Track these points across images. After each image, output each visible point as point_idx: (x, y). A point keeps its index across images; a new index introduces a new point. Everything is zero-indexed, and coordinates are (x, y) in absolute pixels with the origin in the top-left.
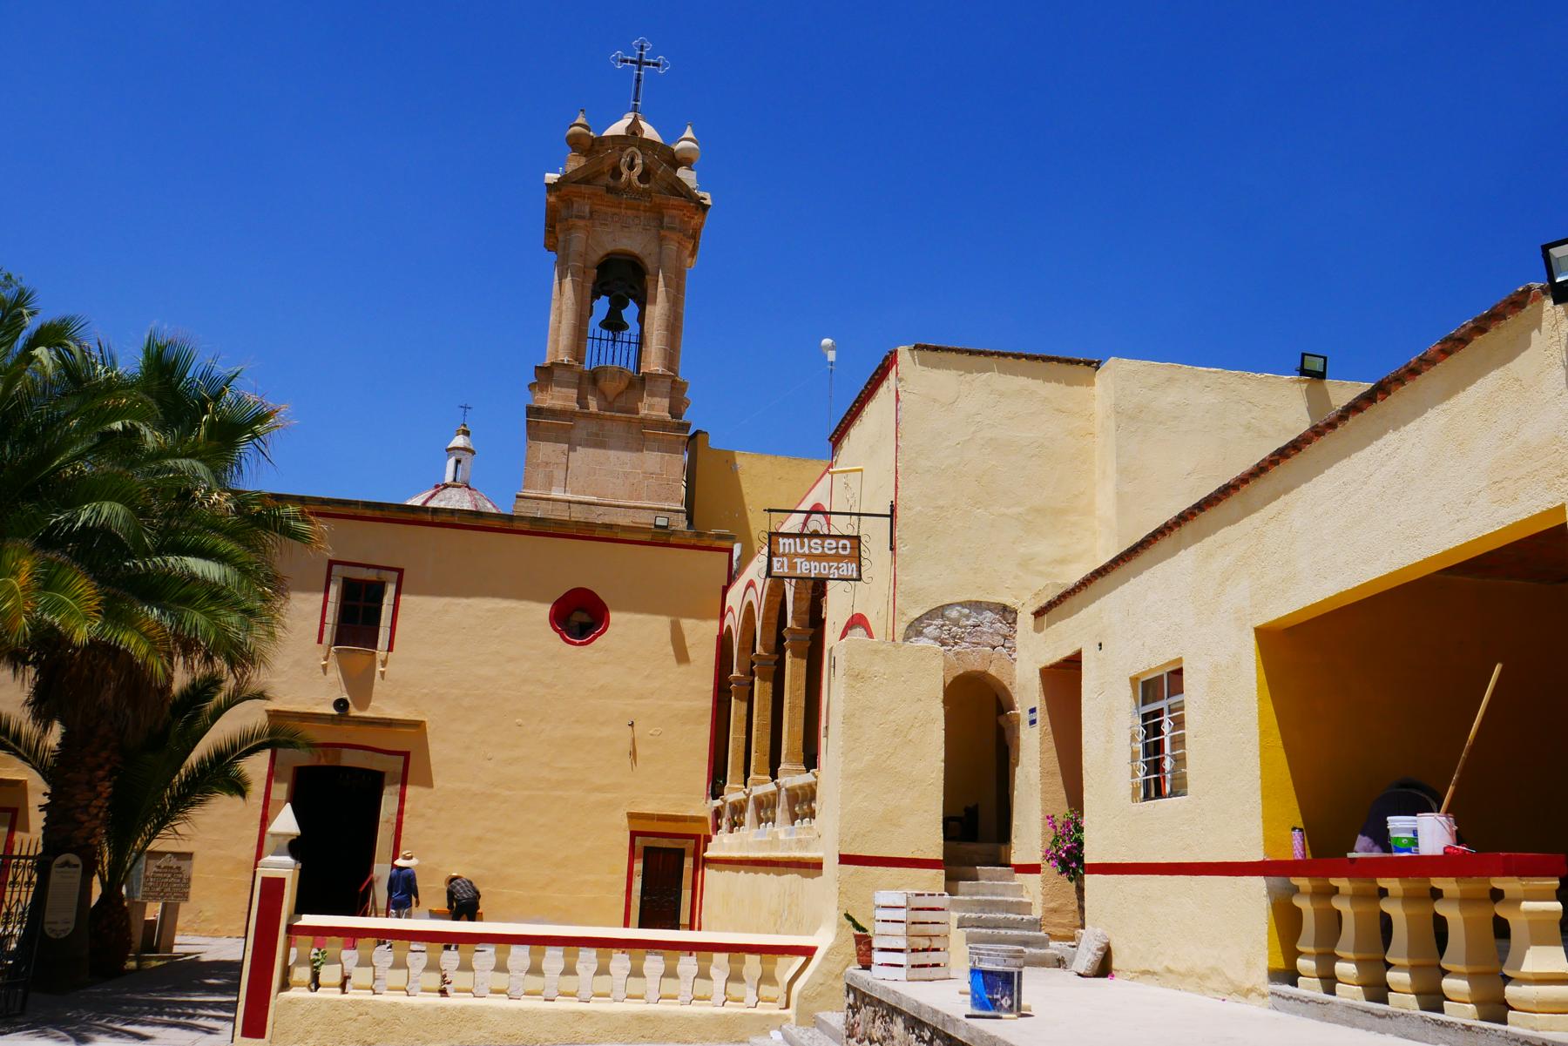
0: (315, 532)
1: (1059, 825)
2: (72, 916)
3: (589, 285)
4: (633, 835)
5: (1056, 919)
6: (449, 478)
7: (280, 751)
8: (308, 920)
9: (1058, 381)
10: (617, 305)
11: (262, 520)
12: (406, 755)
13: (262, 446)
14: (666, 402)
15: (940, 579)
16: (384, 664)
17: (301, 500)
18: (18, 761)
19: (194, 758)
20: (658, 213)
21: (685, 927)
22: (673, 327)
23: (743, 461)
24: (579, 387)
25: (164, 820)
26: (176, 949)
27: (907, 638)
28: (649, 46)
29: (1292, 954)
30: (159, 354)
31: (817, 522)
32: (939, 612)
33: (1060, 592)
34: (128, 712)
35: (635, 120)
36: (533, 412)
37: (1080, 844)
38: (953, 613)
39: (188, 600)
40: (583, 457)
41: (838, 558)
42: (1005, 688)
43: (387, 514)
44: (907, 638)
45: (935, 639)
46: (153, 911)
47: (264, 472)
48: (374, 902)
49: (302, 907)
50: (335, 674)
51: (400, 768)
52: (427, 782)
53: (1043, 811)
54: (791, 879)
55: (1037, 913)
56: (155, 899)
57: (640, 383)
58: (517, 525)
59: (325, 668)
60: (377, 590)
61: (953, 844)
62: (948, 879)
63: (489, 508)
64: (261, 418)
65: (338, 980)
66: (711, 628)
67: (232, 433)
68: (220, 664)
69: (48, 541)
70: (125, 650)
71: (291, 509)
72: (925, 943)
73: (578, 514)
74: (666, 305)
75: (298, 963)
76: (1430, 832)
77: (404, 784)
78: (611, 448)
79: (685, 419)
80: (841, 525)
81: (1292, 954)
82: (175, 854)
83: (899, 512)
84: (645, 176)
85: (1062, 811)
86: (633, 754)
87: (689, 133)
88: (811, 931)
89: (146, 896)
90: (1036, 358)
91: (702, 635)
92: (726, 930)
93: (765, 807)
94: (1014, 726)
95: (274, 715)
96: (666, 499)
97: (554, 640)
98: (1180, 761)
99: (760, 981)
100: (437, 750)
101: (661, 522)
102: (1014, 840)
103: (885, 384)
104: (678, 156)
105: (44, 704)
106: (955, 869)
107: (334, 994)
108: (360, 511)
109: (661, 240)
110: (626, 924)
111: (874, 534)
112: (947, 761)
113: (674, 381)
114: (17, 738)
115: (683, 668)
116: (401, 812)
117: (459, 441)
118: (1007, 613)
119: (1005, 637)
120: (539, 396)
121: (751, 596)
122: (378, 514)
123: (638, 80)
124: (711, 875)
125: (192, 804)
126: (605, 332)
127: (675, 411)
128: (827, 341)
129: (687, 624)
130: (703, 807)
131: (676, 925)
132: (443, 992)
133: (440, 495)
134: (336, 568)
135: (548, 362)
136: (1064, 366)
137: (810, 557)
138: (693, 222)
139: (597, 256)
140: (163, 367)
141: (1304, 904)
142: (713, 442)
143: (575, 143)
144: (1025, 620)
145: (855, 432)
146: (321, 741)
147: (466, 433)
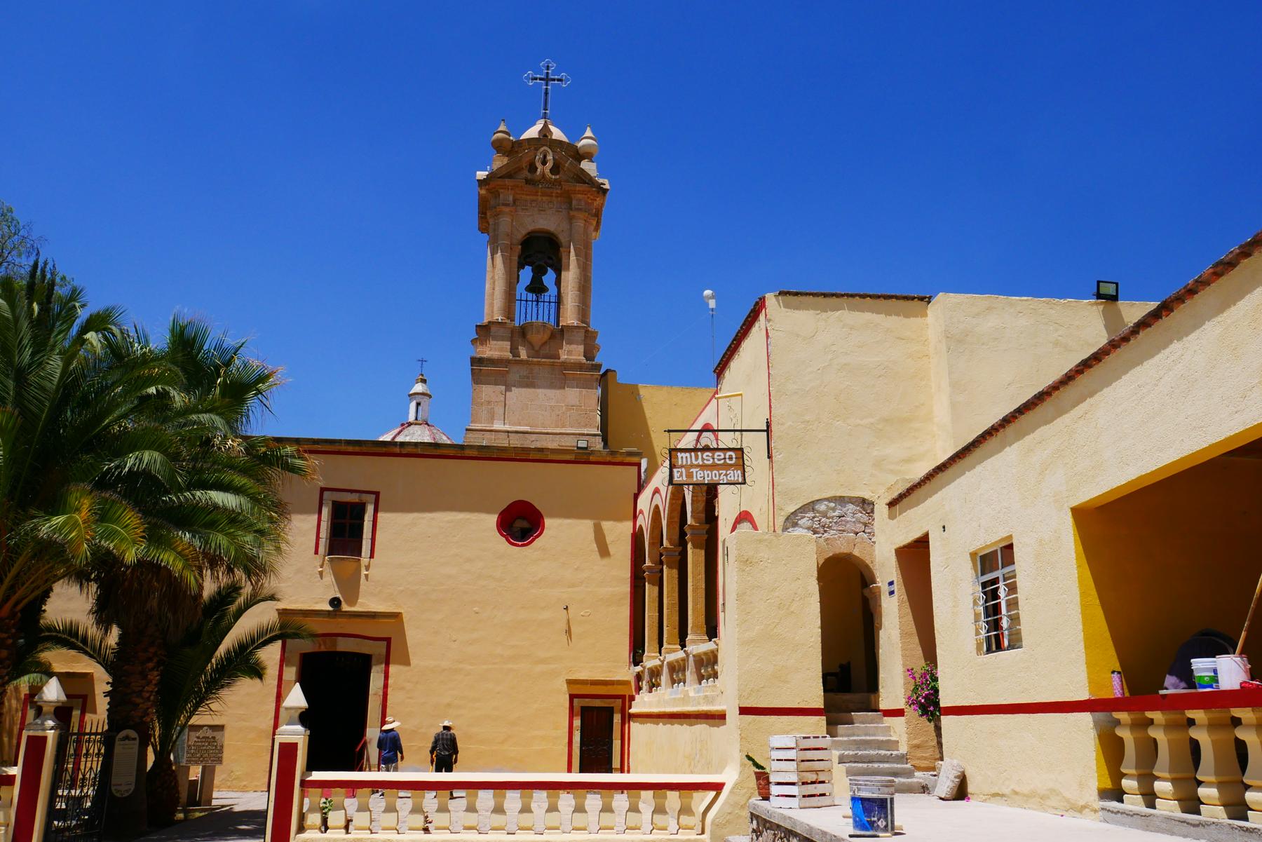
0: (308, 466)
1: (917, 676)
2: (133, 779)
3: (516, 258)
4: (572, 697)
5: (919, 753)
6: (412, 418)
7: (289, 641)
8: (317, 776)
9: (898, 315)
10: (539, 273)
11: (267, 459)
12: (388, 640)
13: (264, 400)
14: (581, 348)
15: (809, 481)
16: (367, 568)
17: (297, 441)
18: (86, 658)
19: (222, 650)
20: (567, 198)
21: (616, 770)
22: (584, 288)
23: (646, 392)
24: (512, 340)
25: (201, 700)
26: (214, 803)
27: (785, 529)
28: (553, 66)
29: (1117, 776)
30: (182, 333)
31: (707, 439)
32: (810, 506)
33: (908, 485)
34: (169, 615)
35: (546, 126)
36: (476, 361)
37: (936, 691)
38: (822, 507)
39: (212, 525)
40: (517, 394)
41: (726, 466)
42: (867, 566)
43: (364, 449)
44: (785, 529)
45: (808, 528)
46: (195, 773)
47: (267, 420)
48: (368, 759)
49: (312, 766)
50: (329, 578)
51: (384, 651)
52: (406, 662)
53: (904, 665)
54: (701, 728)
55: (903, 749)
56: (196, 763)
57: (559, 334)
58: (468, 453)
59: (321, 573)
60: (361, 508)
61: (831, 695)
62: (829, 723)
63: (444, 440)
64: (263, 378)
65: (343, 823)
66: (627, 528)
67: (241, 392)
68: (239, 573)
69: (102, 483)
70: (165, 567)
71: (289, 449)
72: (812, 777)
73: (516, 442)
74: (577, 271)
75: (311, 810)
76: (1229, 671)
77: (387, 664)
78: (539, 387)
79: (597, 360)
80: (727, 440)
81: (1117, 776)
82: (211, 727)
83: (774, 427)
84: (555, 169)
85: (920, 664)
86: (569, 632)
87: (588, 133)
88: (719, 770)
89: (189, 761)
90: (879, 297)
91: (619, 533)
92: (650, 772)
93: (677, 671)
94: (876, 596)
95: (283, 613)
96: (586, 426)
97: (501, 543)
98: (1015, 619)
99: (681, 812)
100: (413, 635)
101: (582, 444)
102: (881, 690)
103: (757, 324)
104: (581, 152)
105: (105, 612)
106: (835, 715)
107: (341, 834)
108: (343, 448)
109: (571, 219)
110: (569, 771)
111: (754, 446)
112: (823, 627)
113: (587, 331)
114: (84, 640)
115: (606, 561)
116: (386, 686)
117: (419, 388)
118: (866, 505)
119: (865, 525)
120: (480, 349)
121: (657, 500)
122: (357, 449)
123: (546, 93)
124: (635, 728)
125: (222, 687)
126: (530, 295)
127: (589, 355)
128: (708, 292)
129: (606, 525)
130: (627, 673)
131: (609, 770)
132: (426, 830)
133: (406, 432)
134: (326, 494)
135: (486, 321)
136: (901, 302)
137: (703, 467)
138: (595, 204)
139: (521, 234)
140: (185, 343)
141: (1125, 734)
142: (622, 378)
143: (499, 146)
144: (881, 510)
145: (734, 364)
146: (320, 631)
147: (424, 381)
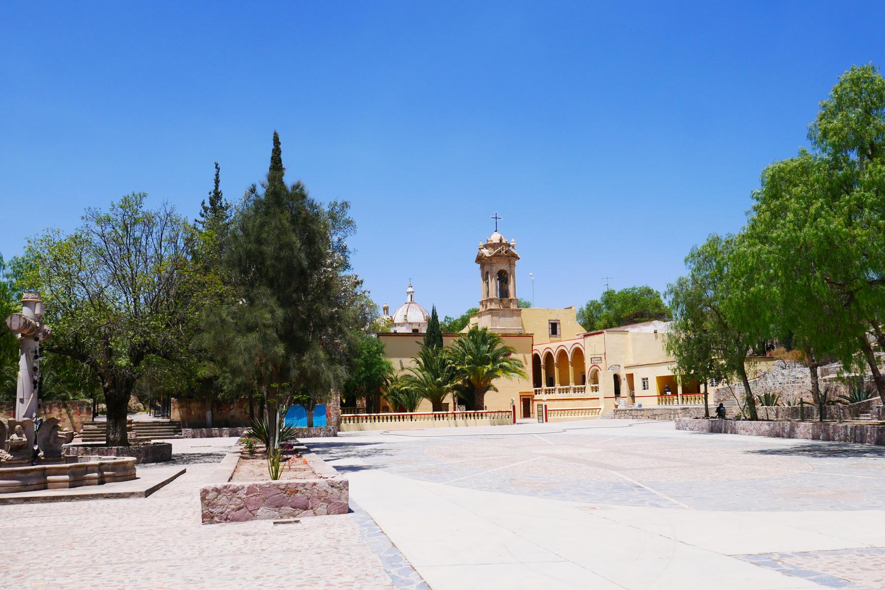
15: (611, 362)
20: (510, 261)
76: (669, 393)
84: (506, 252)
111: (603, 356)
117: (410, 289)
